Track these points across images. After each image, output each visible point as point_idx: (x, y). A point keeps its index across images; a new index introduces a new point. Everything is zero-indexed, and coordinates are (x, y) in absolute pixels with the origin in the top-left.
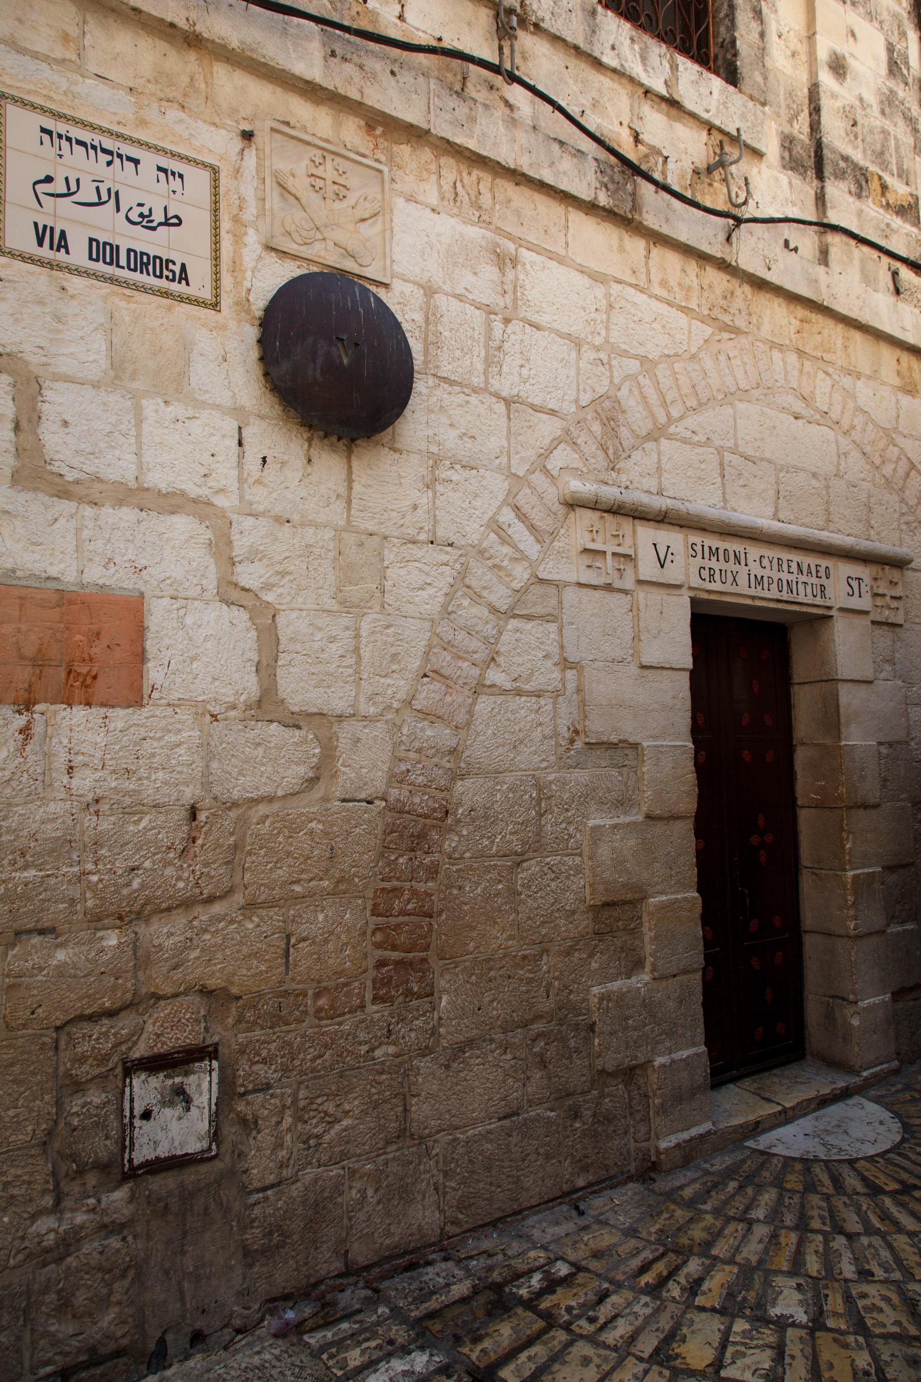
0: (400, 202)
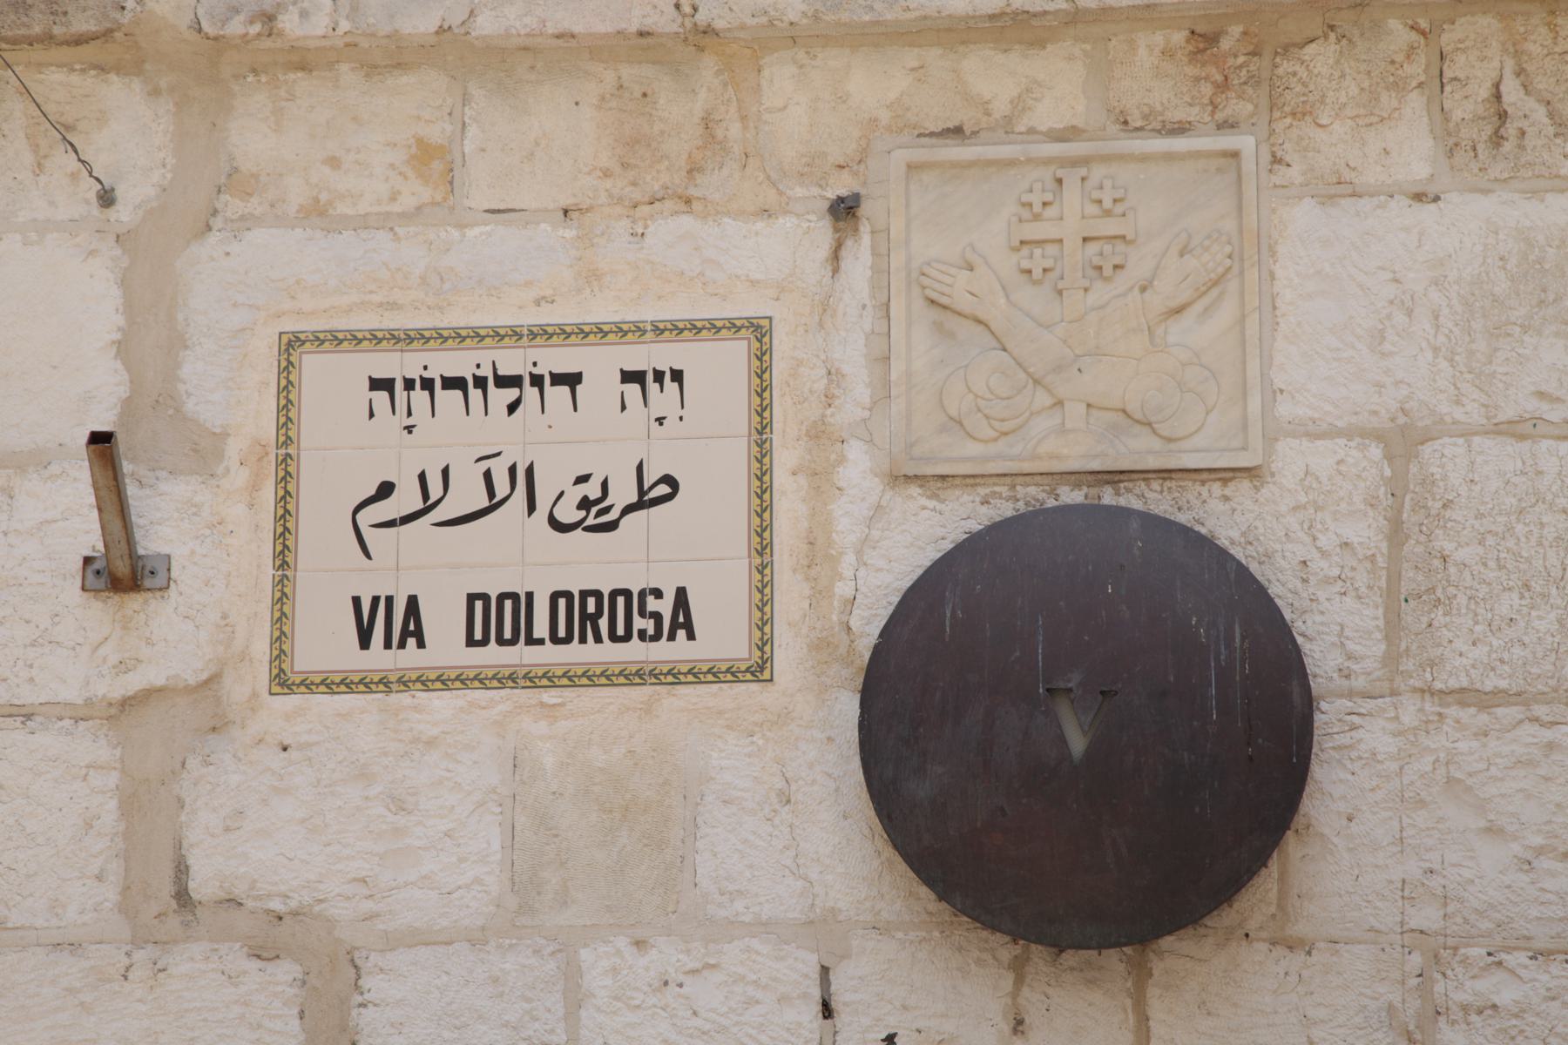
0: (1303, 217)
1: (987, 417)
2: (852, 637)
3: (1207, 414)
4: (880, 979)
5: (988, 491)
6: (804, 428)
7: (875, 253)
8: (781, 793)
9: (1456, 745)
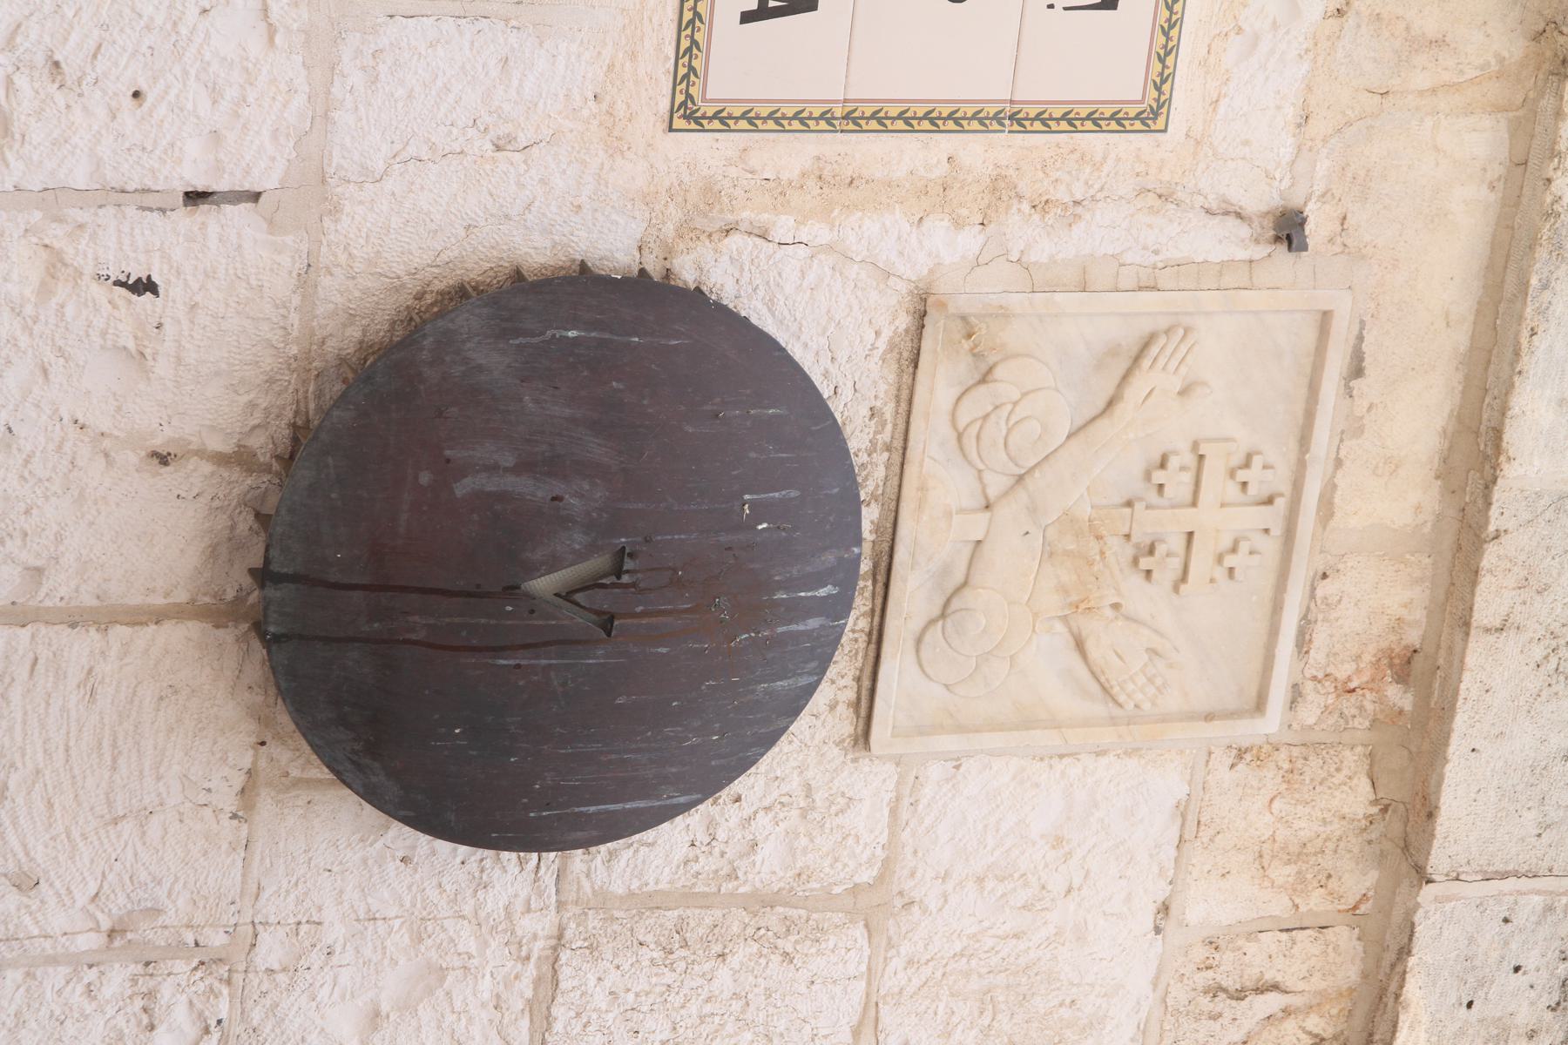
0: (1170, 784)
1: (986, 417)
2: (715, 237)
3: (946, 686)
4: (235, 274)
5: (888, 416)
6: (1011, 172)
7: (1224, 266)
8: (511, 139)
9: (488, 976)
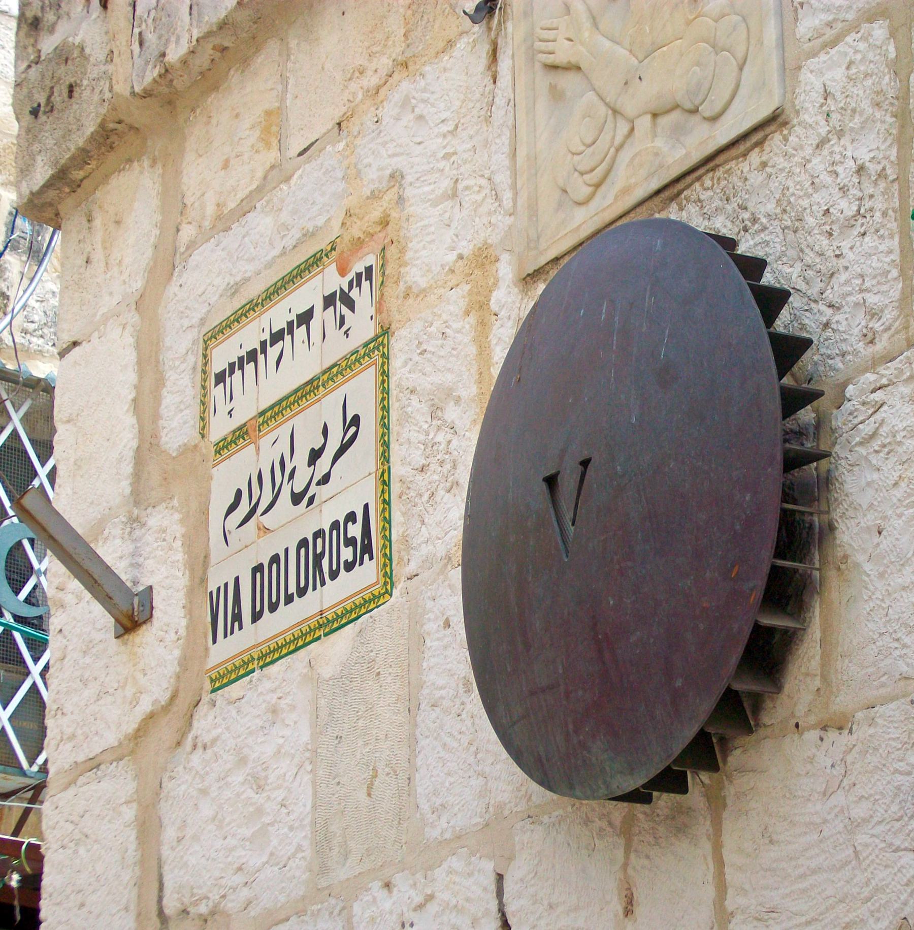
3: (741, 69)
